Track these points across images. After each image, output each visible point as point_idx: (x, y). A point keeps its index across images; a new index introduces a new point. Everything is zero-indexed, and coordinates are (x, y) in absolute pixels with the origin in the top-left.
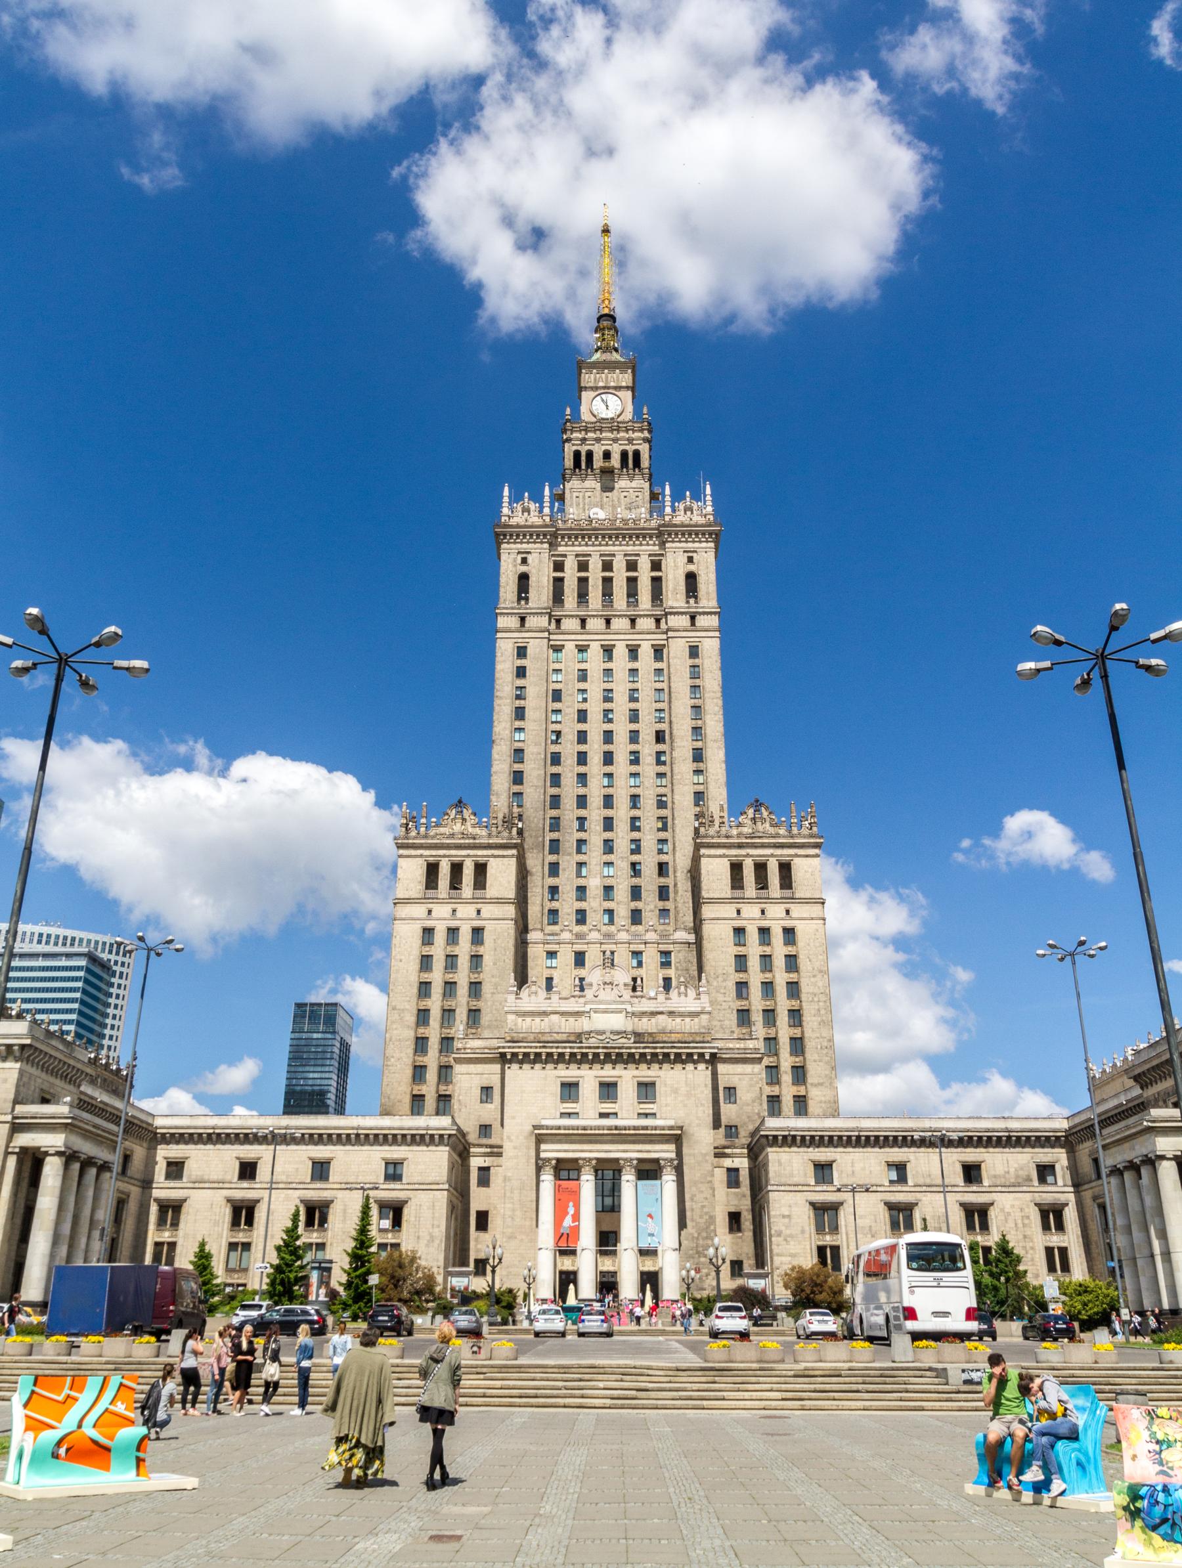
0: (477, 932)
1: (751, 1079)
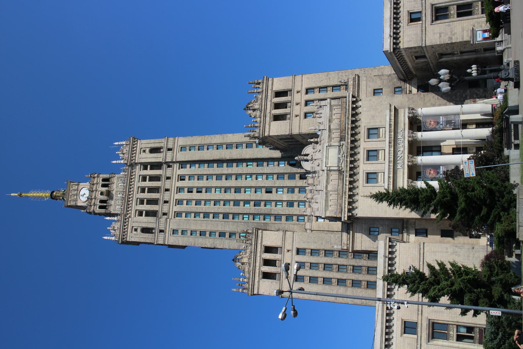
0: (299, 251)
1: (370, 81)
